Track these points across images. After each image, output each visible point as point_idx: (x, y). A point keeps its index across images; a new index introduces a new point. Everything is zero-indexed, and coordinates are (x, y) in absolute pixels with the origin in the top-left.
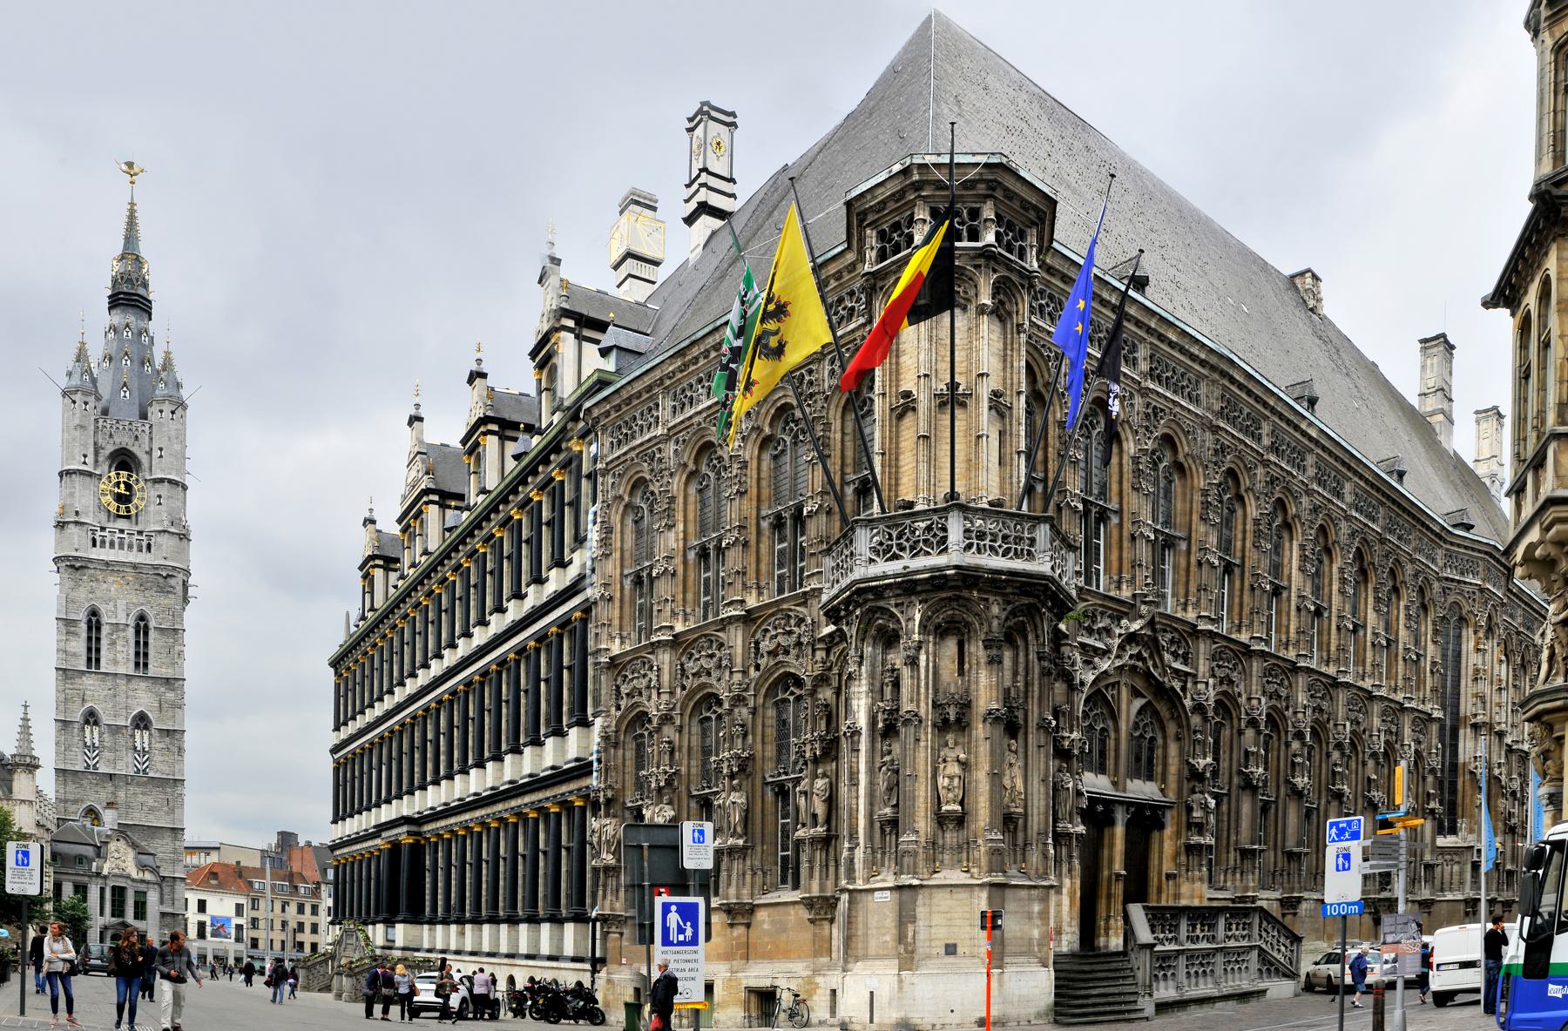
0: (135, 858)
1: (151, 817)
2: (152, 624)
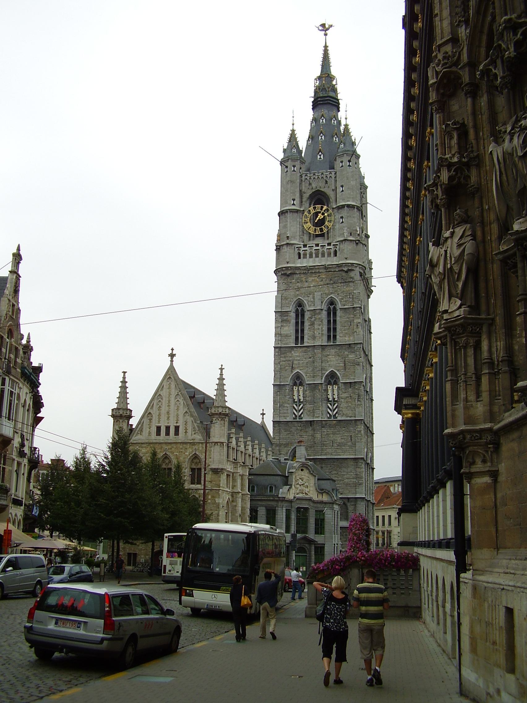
2: (339, 306)
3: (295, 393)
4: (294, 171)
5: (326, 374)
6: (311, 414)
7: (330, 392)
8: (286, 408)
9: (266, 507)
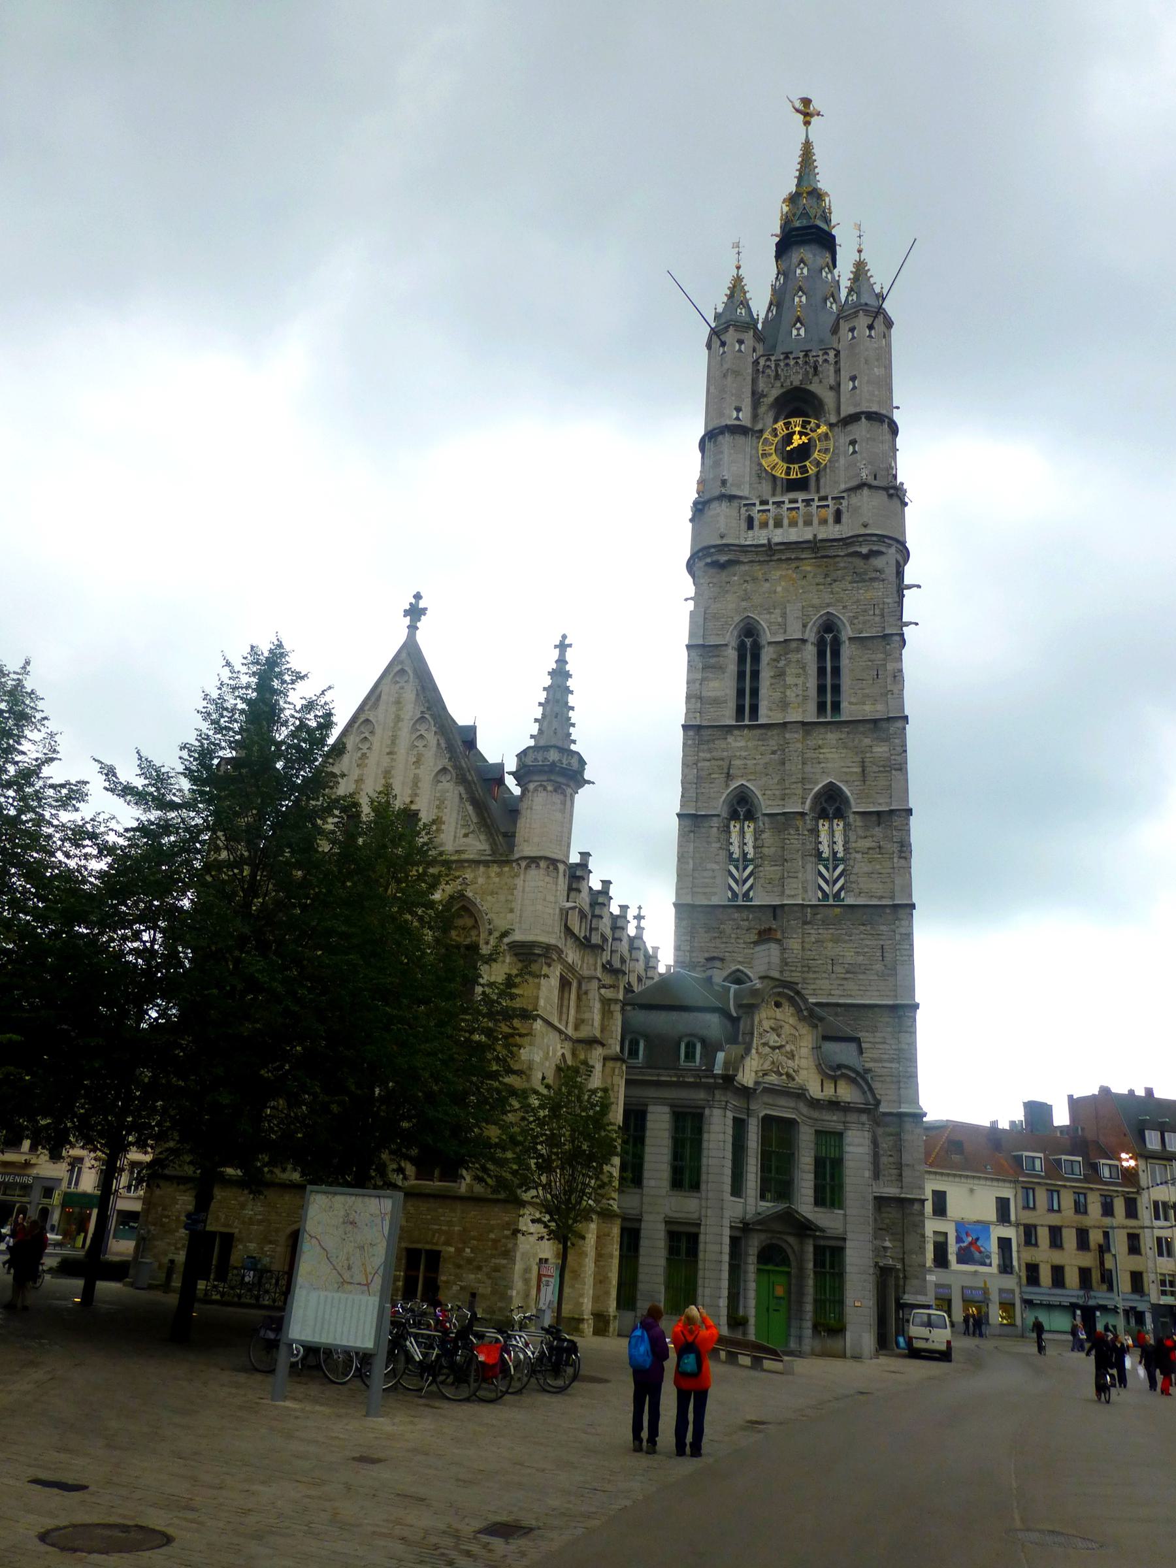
0: (817, 1048)
1: (850, 985)
2: (847, 632)
3: (735, 838)
4: (740, 351)
5: (816, 789)
6: (776, 889)
7: (824, 837)
8: (710, 874)
9: (671, 1106)
